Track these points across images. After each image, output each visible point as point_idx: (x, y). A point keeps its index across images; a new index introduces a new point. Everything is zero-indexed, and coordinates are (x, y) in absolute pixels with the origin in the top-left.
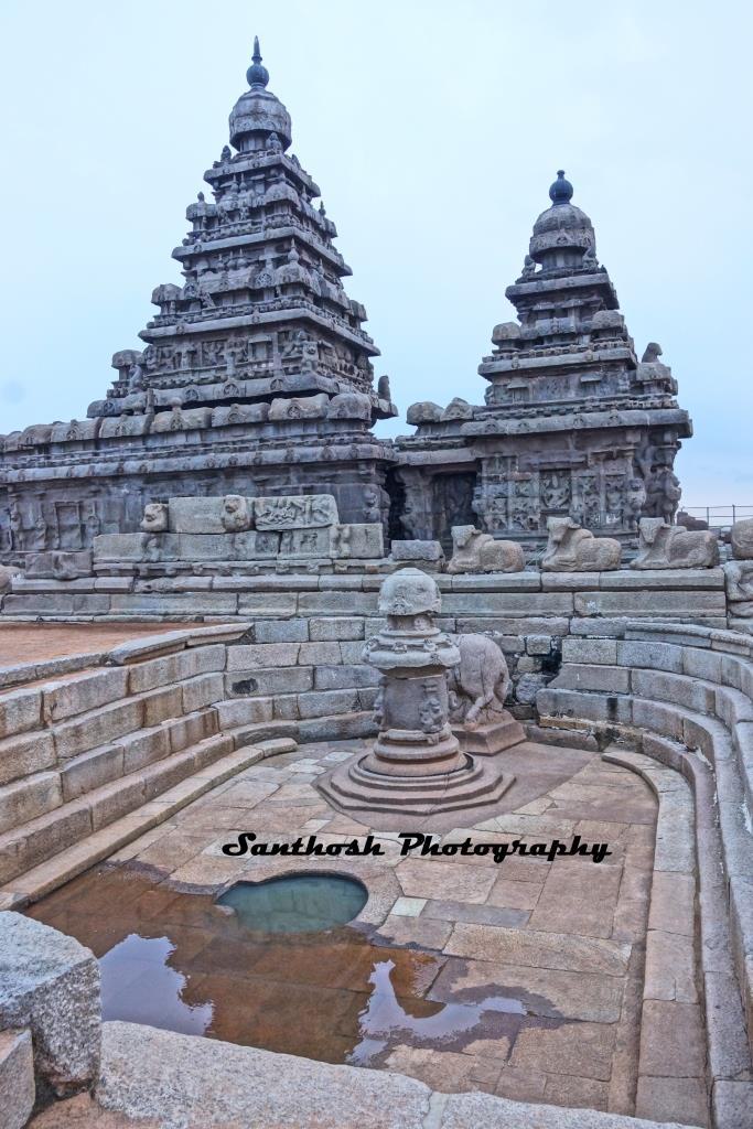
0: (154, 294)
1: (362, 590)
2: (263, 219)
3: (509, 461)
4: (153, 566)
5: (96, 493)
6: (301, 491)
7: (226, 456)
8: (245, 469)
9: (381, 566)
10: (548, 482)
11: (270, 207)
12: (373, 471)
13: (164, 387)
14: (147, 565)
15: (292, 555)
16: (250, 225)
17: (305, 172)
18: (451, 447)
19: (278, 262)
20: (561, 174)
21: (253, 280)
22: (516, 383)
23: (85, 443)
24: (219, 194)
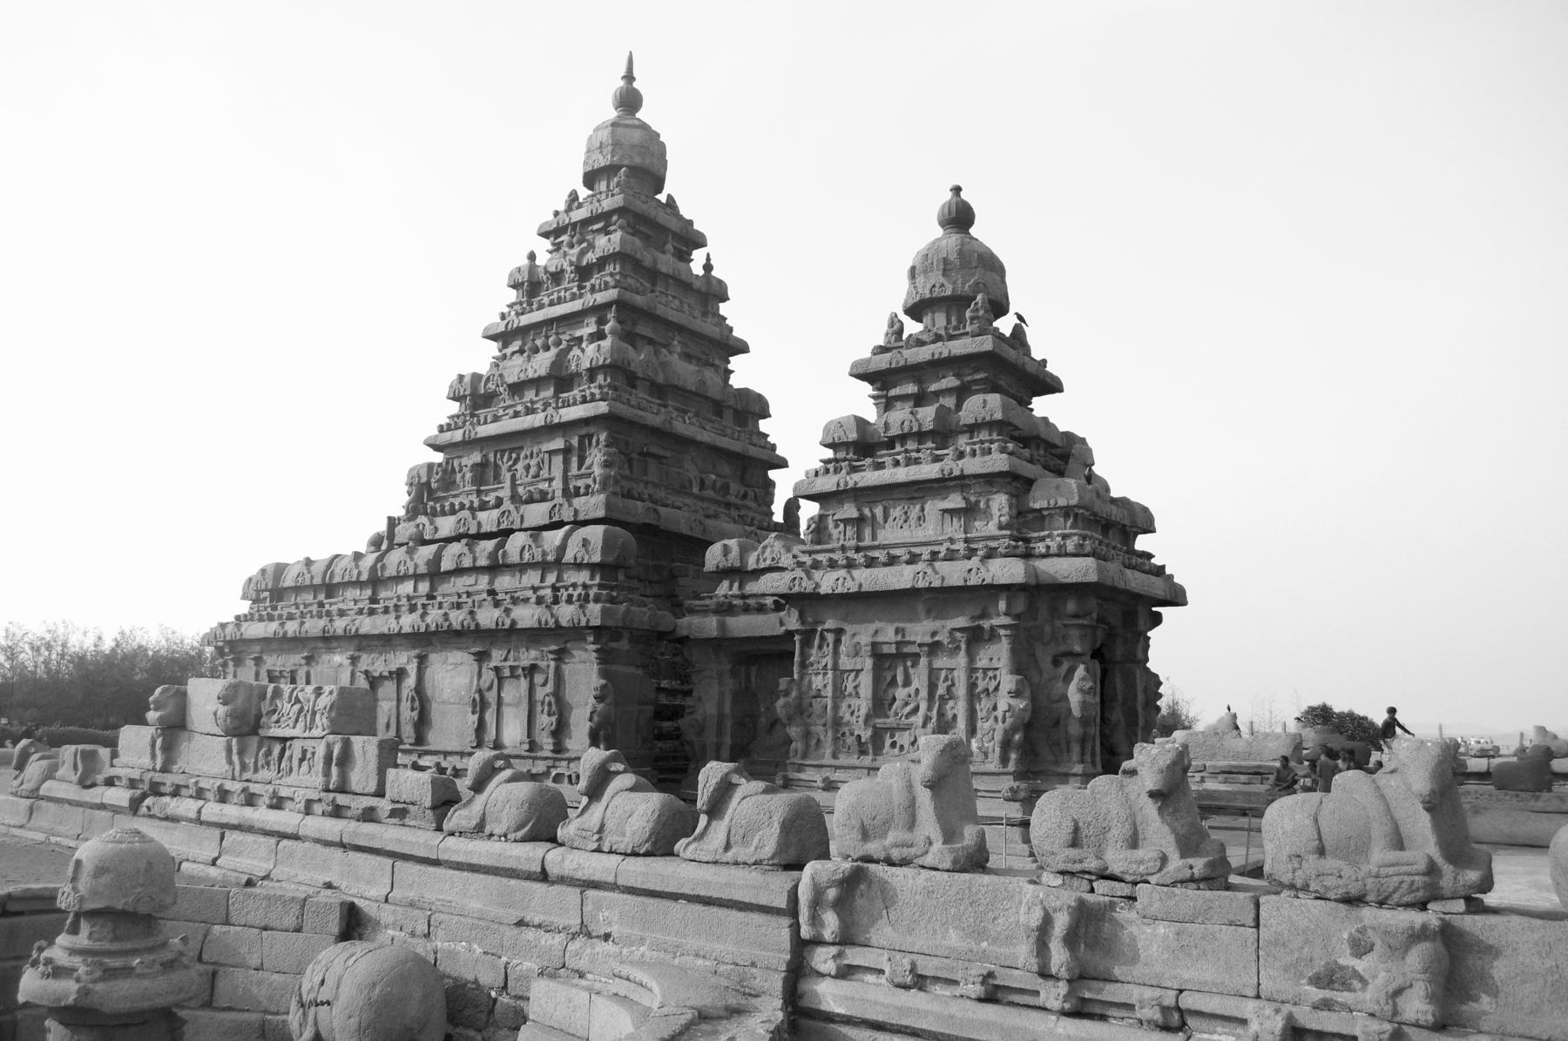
0: (451, 387)
1: (342, 845)
3: (830, 637)
4: (158, 777)
6: (520, 671)
7: (434, 616)
9: (372, 809)
10: (889, 678)
11: (602, 263)
12: (624, 645)
14: (152, 774)
15: (289, 780)
16: (575, 290)
17: (680, 218)
18: (761, 609)
19: (599, 336)
21: (559, 362)
22: (849, 511)
23: (314, 589)
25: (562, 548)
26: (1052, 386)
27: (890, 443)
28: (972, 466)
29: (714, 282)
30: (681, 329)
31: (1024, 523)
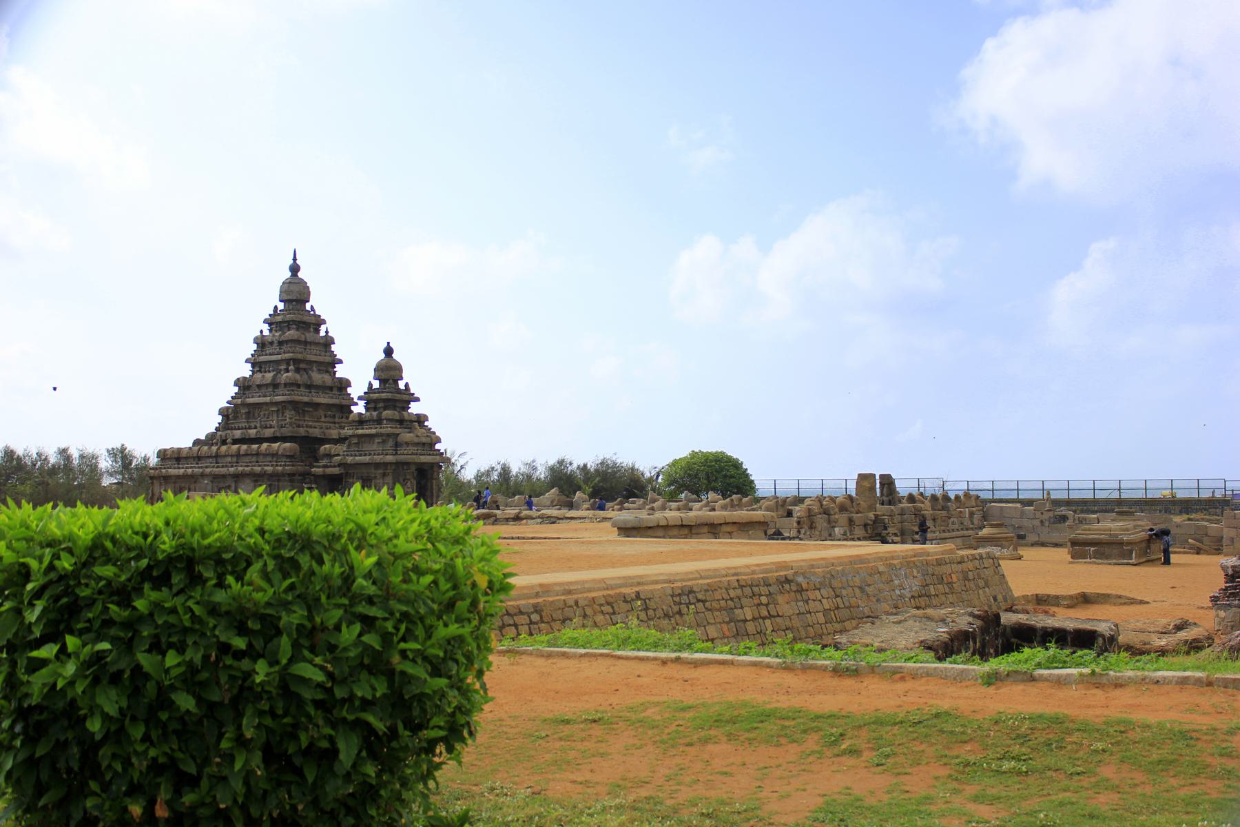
2: (284, 347)
5: (195, 482)
8: (248, 475)
11: (287, 342)
13: (235, 429)
18: (335, 466)
19: (287, 370)
20: (388, 343)
22: (355, 440)
23: (194, 458)
24: (270, 331)
25: (278, 450)
26: (418, 400)
27: (367, 421)
28: (383, 431)
29: (329, 339)
30: (316, 362)
31: (397, 445)
